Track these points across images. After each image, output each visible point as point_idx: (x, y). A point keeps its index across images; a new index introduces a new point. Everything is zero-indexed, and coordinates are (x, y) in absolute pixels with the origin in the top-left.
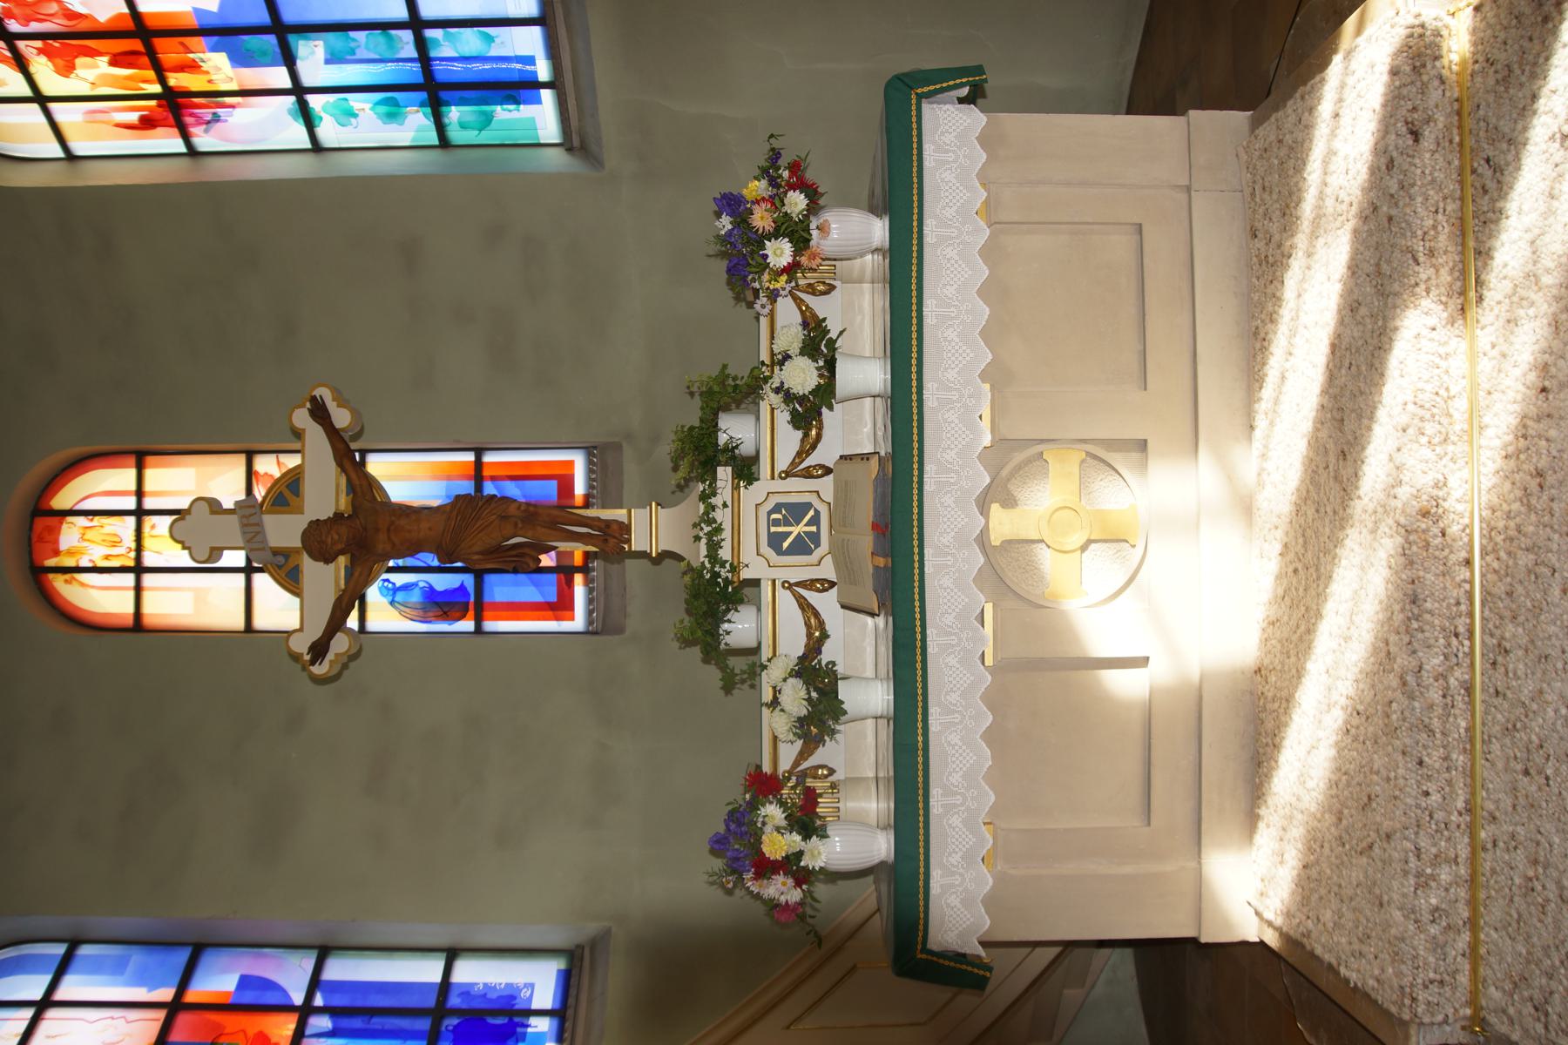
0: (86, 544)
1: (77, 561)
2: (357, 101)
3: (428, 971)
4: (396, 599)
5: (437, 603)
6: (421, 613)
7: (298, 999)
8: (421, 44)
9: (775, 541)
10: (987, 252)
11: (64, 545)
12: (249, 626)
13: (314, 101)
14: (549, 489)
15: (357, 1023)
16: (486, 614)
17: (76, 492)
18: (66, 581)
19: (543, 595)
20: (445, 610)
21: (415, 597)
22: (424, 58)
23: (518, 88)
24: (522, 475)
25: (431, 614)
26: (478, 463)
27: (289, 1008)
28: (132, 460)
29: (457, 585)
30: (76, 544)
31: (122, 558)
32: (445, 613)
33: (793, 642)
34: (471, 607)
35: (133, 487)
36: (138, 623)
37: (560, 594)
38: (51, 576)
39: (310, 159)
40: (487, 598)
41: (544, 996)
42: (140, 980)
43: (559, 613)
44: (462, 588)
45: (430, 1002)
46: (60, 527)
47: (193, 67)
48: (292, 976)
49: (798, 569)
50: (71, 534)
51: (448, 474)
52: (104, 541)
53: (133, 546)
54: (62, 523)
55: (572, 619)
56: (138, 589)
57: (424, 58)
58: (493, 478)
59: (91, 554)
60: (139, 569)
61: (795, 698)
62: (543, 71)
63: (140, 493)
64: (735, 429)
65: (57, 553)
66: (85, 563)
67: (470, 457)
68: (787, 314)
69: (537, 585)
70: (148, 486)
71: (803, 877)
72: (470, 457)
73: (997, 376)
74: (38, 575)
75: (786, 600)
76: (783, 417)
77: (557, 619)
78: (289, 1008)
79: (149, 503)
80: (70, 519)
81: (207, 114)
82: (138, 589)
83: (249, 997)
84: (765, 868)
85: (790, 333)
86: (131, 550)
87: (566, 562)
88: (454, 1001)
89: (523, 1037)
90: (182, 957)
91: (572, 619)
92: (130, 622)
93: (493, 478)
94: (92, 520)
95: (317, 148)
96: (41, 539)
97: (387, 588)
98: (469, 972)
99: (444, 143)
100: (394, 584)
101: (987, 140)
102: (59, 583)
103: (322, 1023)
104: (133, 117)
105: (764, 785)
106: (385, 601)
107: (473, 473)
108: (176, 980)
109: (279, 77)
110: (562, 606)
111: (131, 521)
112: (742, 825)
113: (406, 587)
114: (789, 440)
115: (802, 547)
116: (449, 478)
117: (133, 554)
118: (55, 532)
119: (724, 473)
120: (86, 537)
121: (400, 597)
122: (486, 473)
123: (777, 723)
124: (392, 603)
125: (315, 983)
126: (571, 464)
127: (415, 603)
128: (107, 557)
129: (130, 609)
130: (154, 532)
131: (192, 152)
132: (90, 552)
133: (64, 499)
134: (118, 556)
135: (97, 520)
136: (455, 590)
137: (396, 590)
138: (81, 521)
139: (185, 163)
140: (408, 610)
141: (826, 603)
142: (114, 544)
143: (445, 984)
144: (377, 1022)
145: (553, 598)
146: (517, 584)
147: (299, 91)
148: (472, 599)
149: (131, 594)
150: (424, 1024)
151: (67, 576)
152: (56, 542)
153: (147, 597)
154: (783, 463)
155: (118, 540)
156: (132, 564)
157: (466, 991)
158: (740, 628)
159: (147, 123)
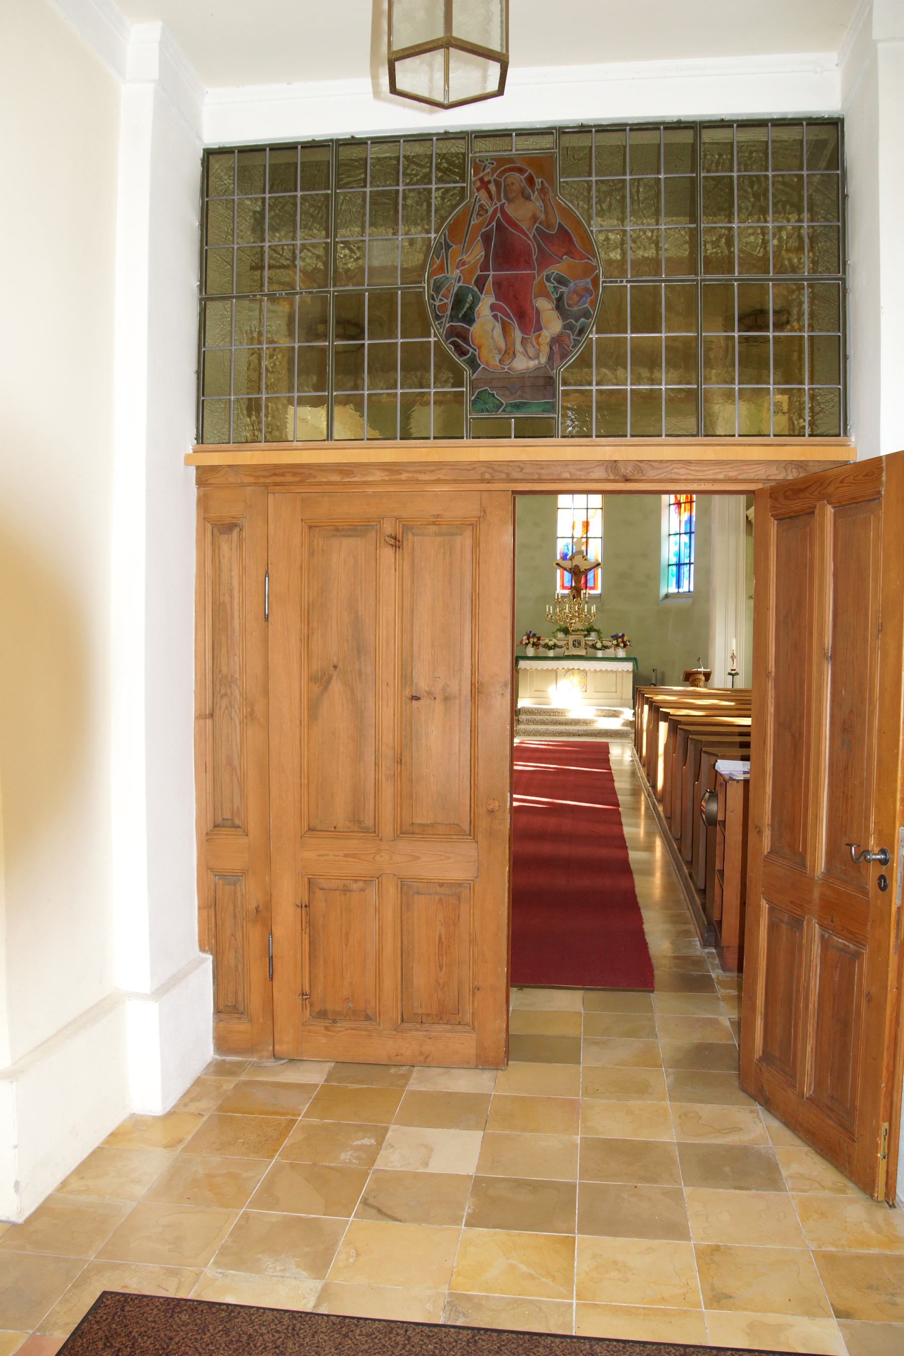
8: (687, 564)
9: (575, 641)
10: (612, 671)
14: (591, 584)
21: (566, 551)
22: (684, 564)
23: (678, 586)
33: (559, 643)
49: (571, 643)
57: (684, 564)
61: (551, 643)
62: (681, 590)
64: (593, 634)
68: (609, 644)
71: (527, 644)
73: (595, 671)
75: (565, 642)
76: (593, 642)
84: (528, 639)
85: (606, 643)
99: (669, 565)
101: (628, 671)
105: (539, 639)
109: (683, 531)
110: (563, 587)
112: (534, 635)
114: (590, 643)
115: (574, 645)
119: (586, 633)
123: (547, 641)
131: (670, 505)
141: (564, 649)
147: (680, 534)
154: (587, 642)
158: (560, 635)
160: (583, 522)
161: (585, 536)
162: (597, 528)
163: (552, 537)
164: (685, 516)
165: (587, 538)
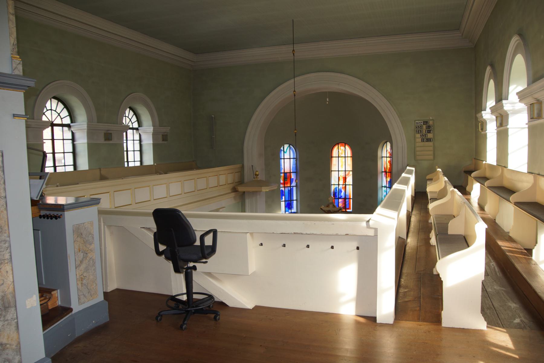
2: (385, 193)
3: (295, 198)
7: (291, 186)
12: (332, 171)
13: (386, 188)
15: (289, 192)
17: (347, 148)
21: (335, 191)
24: (349, 204)
26: (351, 199)
27: (291, 185)
36: (332, 157)
39: (381, 186)
41: (293, 211)
42: (293, 168)
44: (336, 197)
45: (292, 199)
47: (388, 177)
48: (294, 184)
50: (343, 148)
51: (350, 195)
56: (336, 157)
58: (349, 201)
60: (338, 157)
63: (347, 157)
65: (340, 146)
67: (351, 198)
70: (348, 158)
74: (338, 144)
78: (291, 185)
79: (346, 158)
81: (385, 175)
82: (336, 157)
83: (291, 180)
88: (292, 202)
89: (289, 210)
90: (295, 171)
92: (332, 156)
95: (382, 187)
96: (342, 144)
98: (295, 202)
102: (337, 147)
103: (289, 189)
104: (385, 167)
106: (335, 187)
108: (293, 172)
111: (344, 156)
113: (337, 190)
118: (343, 146)
121: (336, 189)
125: (293, 186)
126: (350, 209)
129: (334, 156)
133: (347, 147)
135: (344, 151)
139: (381, 171)
142: (341, 154)
143: (293, 200)
144: (290, 194)
149: (335, 156)
150: (290, 199)
152: (342, 146)
153: (335, 158)
157: (293, 203)
159: (385, 168)
160: (343, 177)
161: (344, 184)
162: (350, 180)
163: (329, 184)
164: (388, 179)
165: (346, 185)
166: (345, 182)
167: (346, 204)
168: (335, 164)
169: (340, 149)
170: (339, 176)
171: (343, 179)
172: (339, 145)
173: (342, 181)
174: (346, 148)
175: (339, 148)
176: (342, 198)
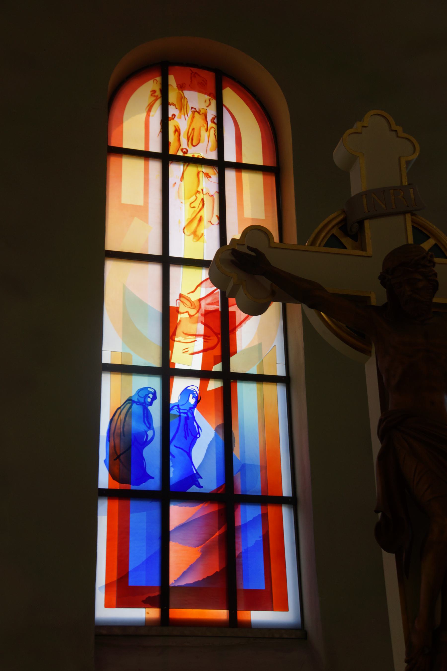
0: (190, 114)
1: (173, 104)
4: (134, 405)
5: (129, 448)
6: (118, 431)
11: (188, 94)
16: (116, 503)
18: (154, 92)
19: (136, 569)
20: (122, 457)
25: (117, 441)
28: (271, 163)
29: (149, 471)
30: (190, 105)
31: (177, 144)
32: (118, 457)
34: (125, 486)
35: (245, 160)
37: (137, 590)
38: (159, 79)
40: (133, 504)
43: (115, 589)
44: (147, 477)
46: (205, 93)
52: (193, 129)
53: (189, 155)
54: (209, 95)
55: (108, 605)
58: (264, 516)
59: (180, 117)
65: (181, 87)
66: (172, 110)
67: (286, 491)
69: (148, 560)
70: (246, 176)
72: (286, 491)
77: (108, 586)
79: (230, 175)
80: (214, 102)
86: (185, 153)
87: (173, 599)
91: (108, 605)
93: (264, 516)
94: (213, 122)
97: (147, 396)
100: (151, 404)
106: (133, 392)
107: (270, 494)
113: (147, 417)
116: (264, 468)
117: (180, 154)
120: (196, 114)
121: (137, 409)
122: (271, 509)
124: (130, 400)
127: (130, 425)
128: (177, 131)
129: (126, 145)
130: (201, 175)
132: (183, 117)
134: (179, 140)
136: (144, 469)
137: (145, 406)
138: (212, 113)
140: (122, 416)
142: (190, 139)
145: (132, 582)
146: (149, 538)
148: (133, 487)
149: (141, 147)
151: (158, 93)
152: (192, 88)
155: (194, 143)
156: (172, 151)
160: (207, 313)
166: (217, 352)
167: (240, 548)
168: (140, 202)
169: (182, 106)
170: (173, 303)
171: (201, 329)
172: (172, 80)
173: (200, 344)
174: (226, 101)
175: (173, 96)
176: (194, 489)
